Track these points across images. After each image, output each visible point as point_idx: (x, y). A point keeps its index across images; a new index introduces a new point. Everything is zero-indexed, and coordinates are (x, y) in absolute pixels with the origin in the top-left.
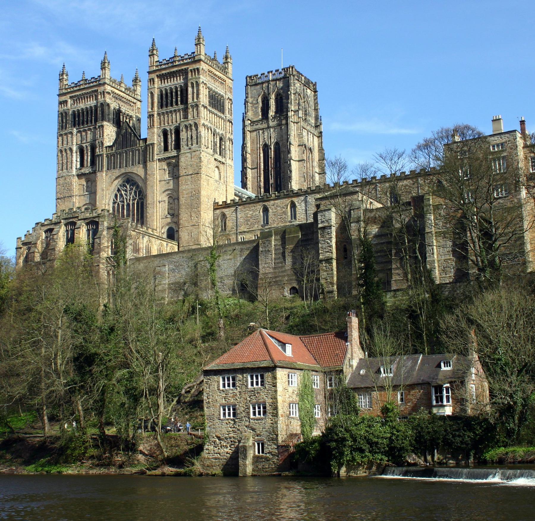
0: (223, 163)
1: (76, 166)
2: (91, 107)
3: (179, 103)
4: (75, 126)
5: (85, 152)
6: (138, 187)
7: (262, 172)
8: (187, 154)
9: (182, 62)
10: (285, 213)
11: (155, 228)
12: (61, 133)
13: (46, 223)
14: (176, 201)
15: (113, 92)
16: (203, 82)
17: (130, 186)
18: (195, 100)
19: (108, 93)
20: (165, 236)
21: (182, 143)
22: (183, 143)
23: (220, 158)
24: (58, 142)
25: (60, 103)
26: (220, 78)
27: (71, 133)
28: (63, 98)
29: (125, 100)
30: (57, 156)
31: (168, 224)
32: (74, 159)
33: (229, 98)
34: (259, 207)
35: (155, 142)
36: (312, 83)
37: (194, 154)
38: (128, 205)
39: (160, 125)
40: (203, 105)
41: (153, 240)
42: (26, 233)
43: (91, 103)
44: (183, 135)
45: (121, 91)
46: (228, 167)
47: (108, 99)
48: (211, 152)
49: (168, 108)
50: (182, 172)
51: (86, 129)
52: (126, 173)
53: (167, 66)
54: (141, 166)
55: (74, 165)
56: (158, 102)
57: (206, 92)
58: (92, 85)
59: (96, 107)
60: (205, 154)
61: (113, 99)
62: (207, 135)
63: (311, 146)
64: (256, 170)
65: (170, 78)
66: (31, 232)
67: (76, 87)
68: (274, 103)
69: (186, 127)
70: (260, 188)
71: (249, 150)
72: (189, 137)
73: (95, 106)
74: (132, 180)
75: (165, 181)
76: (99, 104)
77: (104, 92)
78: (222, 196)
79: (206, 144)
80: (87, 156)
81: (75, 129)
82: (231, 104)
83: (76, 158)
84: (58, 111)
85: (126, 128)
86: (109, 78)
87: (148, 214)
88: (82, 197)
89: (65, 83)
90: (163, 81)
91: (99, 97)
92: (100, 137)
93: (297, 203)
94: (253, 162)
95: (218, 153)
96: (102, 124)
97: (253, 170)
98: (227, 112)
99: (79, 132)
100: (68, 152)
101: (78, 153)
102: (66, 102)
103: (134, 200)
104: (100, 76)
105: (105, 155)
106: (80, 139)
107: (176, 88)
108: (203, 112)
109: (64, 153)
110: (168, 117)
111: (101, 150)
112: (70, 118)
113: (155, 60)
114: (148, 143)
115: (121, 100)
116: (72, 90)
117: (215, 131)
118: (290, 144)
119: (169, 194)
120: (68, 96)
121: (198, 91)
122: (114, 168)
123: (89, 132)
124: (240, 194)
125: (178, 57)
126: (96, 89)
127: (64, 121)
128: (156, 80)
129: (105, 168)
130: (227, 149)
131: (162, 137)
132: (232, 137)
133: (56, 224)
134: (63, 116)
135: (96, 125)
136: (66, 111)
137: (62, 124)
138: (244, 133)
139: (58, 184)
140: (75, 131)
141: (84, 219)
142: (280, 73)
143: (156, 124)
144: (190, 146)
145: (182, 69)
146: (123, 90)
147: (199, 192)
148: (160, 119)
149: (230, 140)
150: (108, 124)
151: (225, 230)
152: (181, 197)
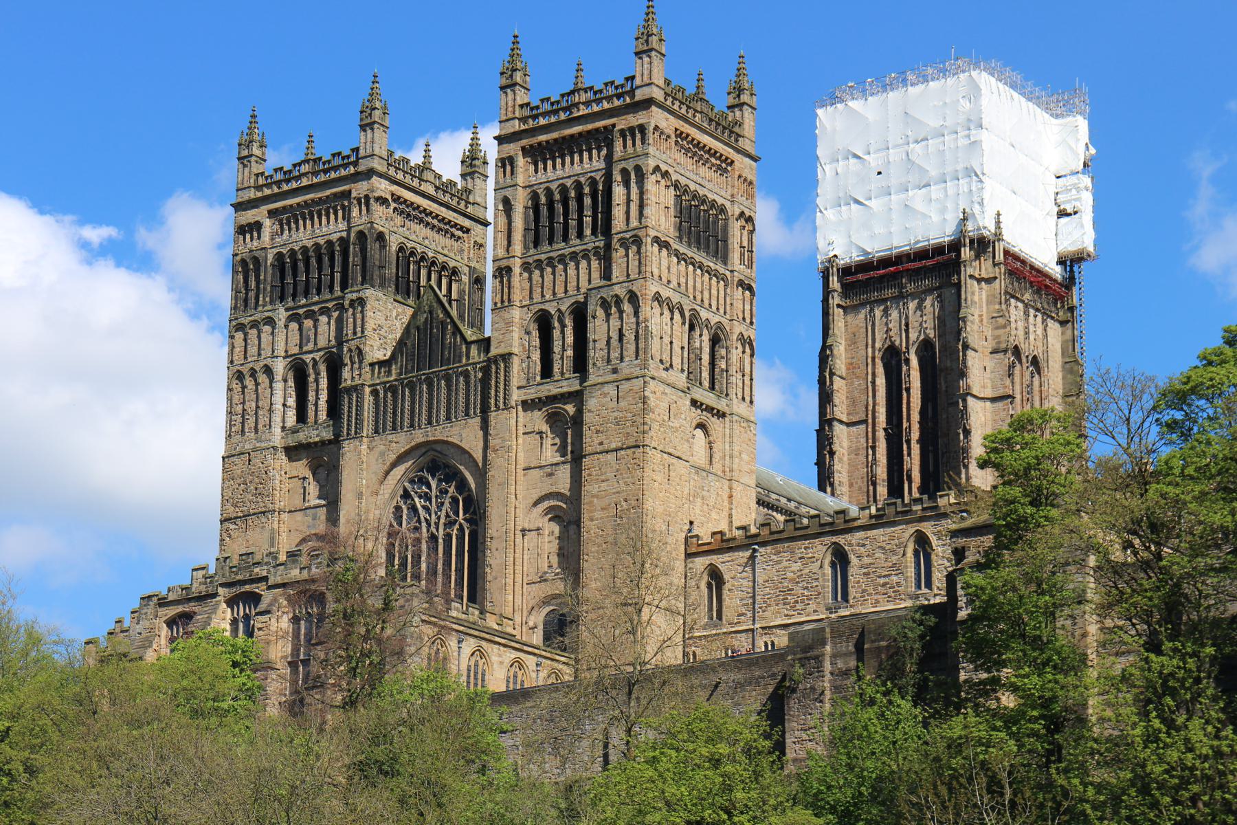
0: (721, 415)
1: (284, 422)
2: (330, 243)
3: (588, 232)
4: (282, 299)
5: (311, 379)
6: (462, 485)
7: (881, 434)
9: (595, 108)
10: (897, 568)
11: (508, 611)
12: (242, 320)
13: (171, 597)
14: (573, 528)
15: (397, 199)
16: (657, 168)
17: (440, 481)
18: (634, 223)
19: (383, 201)
20: (537, 638)
21: (591, 353)
22: (595, 354)
23: (709, 398)
24: (232, 347)
25: (242, 230)
26: (713, 153)
27: (270, 321)
28: (250, 216)
29: (435, 222)
30: (230, 389)
31: (545, 602)
32: (278, 399)
33: (742, 214)
34: (820, 550)
35: (515, 350)
37: (625, 386)
38: (433, 538)
39: (531, 298)
40: (656, 240)
41: (493, 651)
42: (111, 626)
43: (332, 229)
44: (598, 329)
45: (423, 195)
46: (736, 426)
47: (383, 218)
48: (681, 379)
49: (555, 246)
50: (591, 441)
51: (316, 308)
52: (428, 443)
53: (553, 119)
54: (476, 422)
55: (277, 419)
57: (669, 197)
58: (333, 175)
59: (344, 242)
60: (662, 387)
61: (399, 220)
62: (667, 328)
63: (1039, 352)
64: (863, 427)
65: (562, 157)
66: (126, 624)
67: (288, 181)
69: (605, 305)
70: (874, 484)
71: (840, 363)
72: (615, 335)
73: (341, 239)
74: (447, 466)
75: (540, 467)
76: (353, 235)
77: (367, 197)
78: (714, 515)
79: (666, 357)
80: (317, 391)
81: (282, 310)
82: (752, 232)
83: (282, 395)
84: (235, 255)
85: (450, 304)
86: (384, 154)
87: (488, 570)
88: (299, 516)
89: (256, 168)
90: (541, 165)
91: (355, 212)
92: (355, 333)
93: (934, 540)
94: (853, 402)
95: (706, 384)
96: (362, 294)
97: (854, 429)
98: (735, 256)
99: (294, 318)
100: (263, 378)
101: (291, 383)
102: (257, 226)
103: (450, 524)
104: (356, 150)
105: (367, 390)
106: (295, 338)
107: (578, 186)
108: (658, 261)
109: (249, 383)
110: (554, 273)
111: (356, 372)
112: (268, 274)
113: (519, 101)
114: (494, 351)
115: (421, 221)
116: (276, 190)
117: (695, 314)
118: (966, 347)
119: (551, 509)
120: (264, 209)
121: (642, 194)
122: (394, 429)
123: (323, 319)
124: (792, 505)
125: (585, 90)
126: (346, 187)
127: (253, 284)
128: (521, 161)
129: (367, 429)
130: (733, 370)
131: (535, 333)
132: (750, 333)
133: (202, 598)
134: (246, 268)
135: (343, 298)
136: (257, 254)
137: (247, 294)
138: (826, 313)
139: (228, 475)
140: (281, 315)
141: (283, 585)
143: (517, 297)
144: (614, 362)
145: (597, 130)
146: (430, 190)
147: (640, 502)
148: (530, 279)
149: (746, 342)
150: (380, 294)
151: (720, 617)
152: (585, 516)
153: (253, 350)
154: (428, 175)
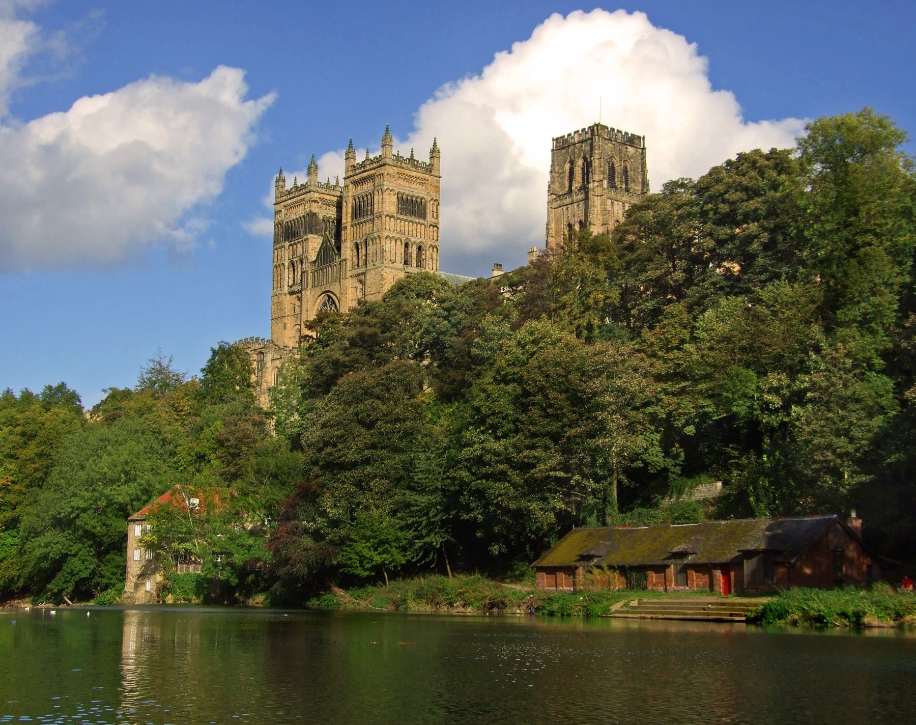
8: (372, 271)
27: (283, 247)
32: (286, 273)
35: (348, 257)
36: (639, 137)
37: (377, 270)
40: (388, 215)
56: (353, 212)
59: (304, 216)
68: (580, 172)
71: (552, 232)
89: (281, 190)
98: (429, 216)
100: (282, 267)
106: (291, 253)
123: (299, 245)
128: (351, 186)
129: (310, 286)
131: (355, 251)
141: (255, 350)
142: (587, 133)
150: (315, 236)
153: (279, 258)
154: (337, 188)
